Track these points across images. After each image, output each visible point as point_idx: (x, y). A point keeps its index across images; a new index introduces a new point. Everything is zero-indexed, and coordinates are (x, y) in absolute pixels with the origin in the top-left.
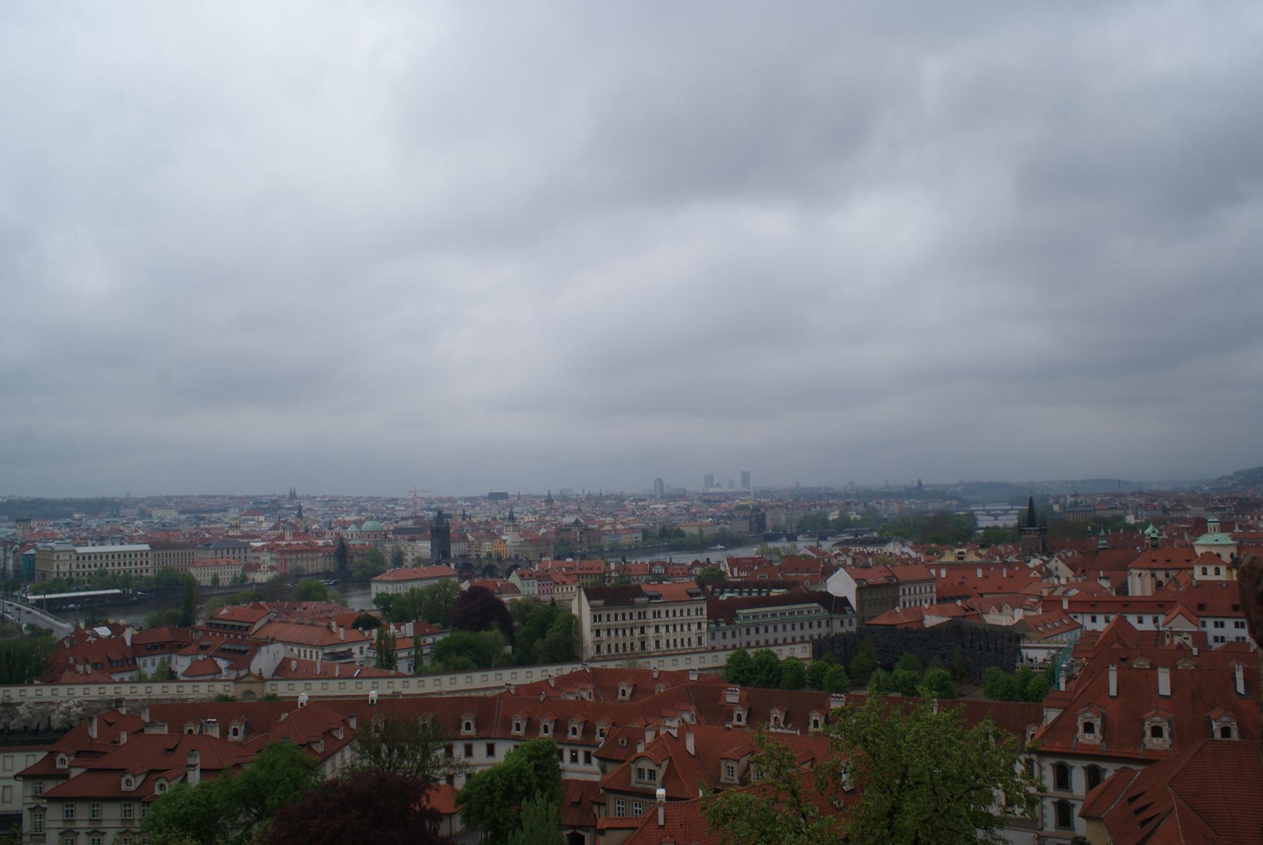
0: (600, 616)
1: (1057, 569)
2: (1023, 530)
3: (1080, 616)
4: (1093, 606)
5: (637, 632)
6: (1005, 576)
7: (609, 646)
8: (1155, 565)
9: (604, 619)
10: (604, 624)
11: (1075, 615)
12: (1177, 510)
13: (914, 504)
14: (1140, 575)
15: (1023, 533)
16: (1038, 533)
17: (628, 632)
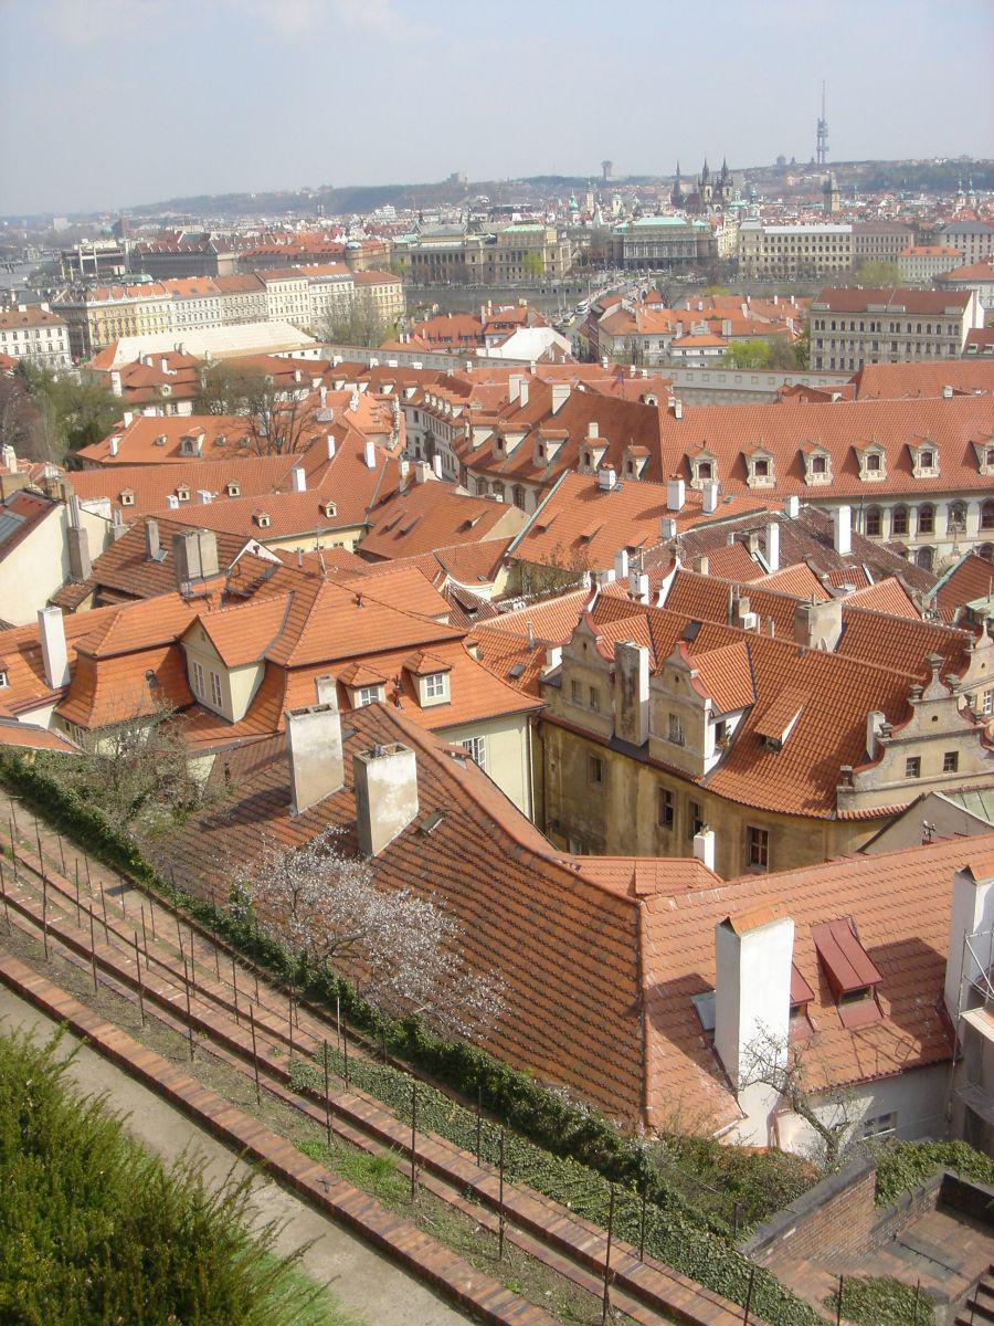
0: (823, 323)
5: (868, 347)
7: (833, 360)
9: (829, 326)
10: (827, 332)
17: (857, 345)
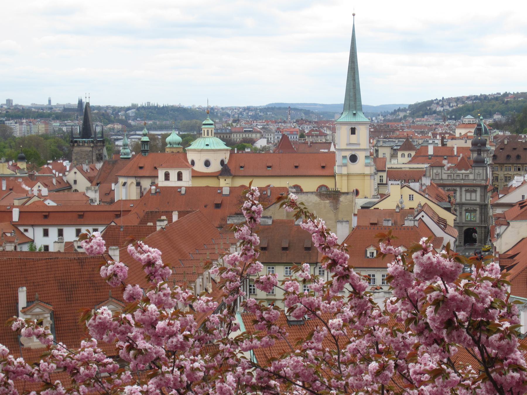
1: (75, 182)
2: (76, 142)
3: (30, 229)
4: (46, 217)
6: (4, 188)
8: (141, 173)
11: (26, 228)
12: (312, 136)
13: (66, 126)
14: (124, 184)
15: (76, 145)
16: (92, 145)
